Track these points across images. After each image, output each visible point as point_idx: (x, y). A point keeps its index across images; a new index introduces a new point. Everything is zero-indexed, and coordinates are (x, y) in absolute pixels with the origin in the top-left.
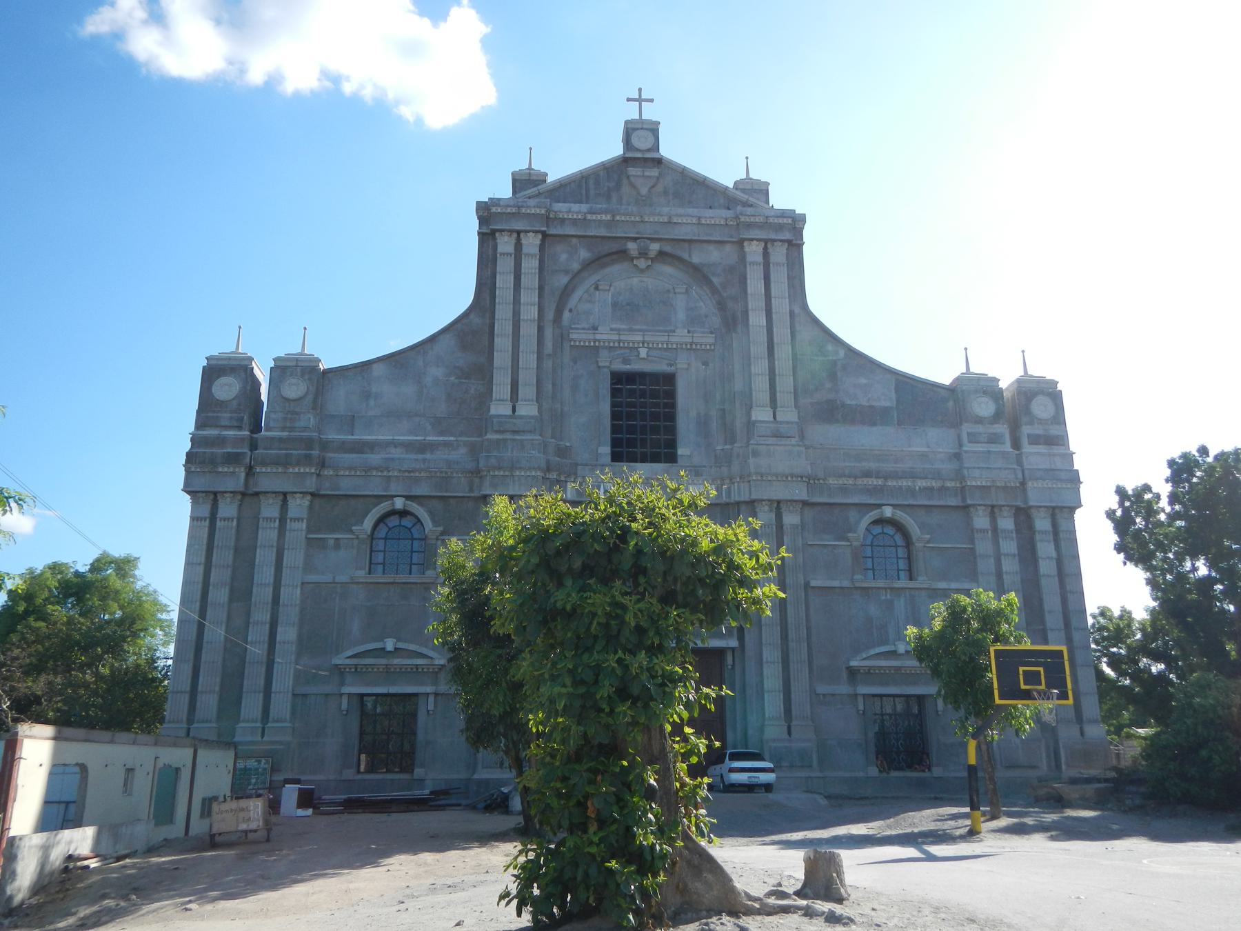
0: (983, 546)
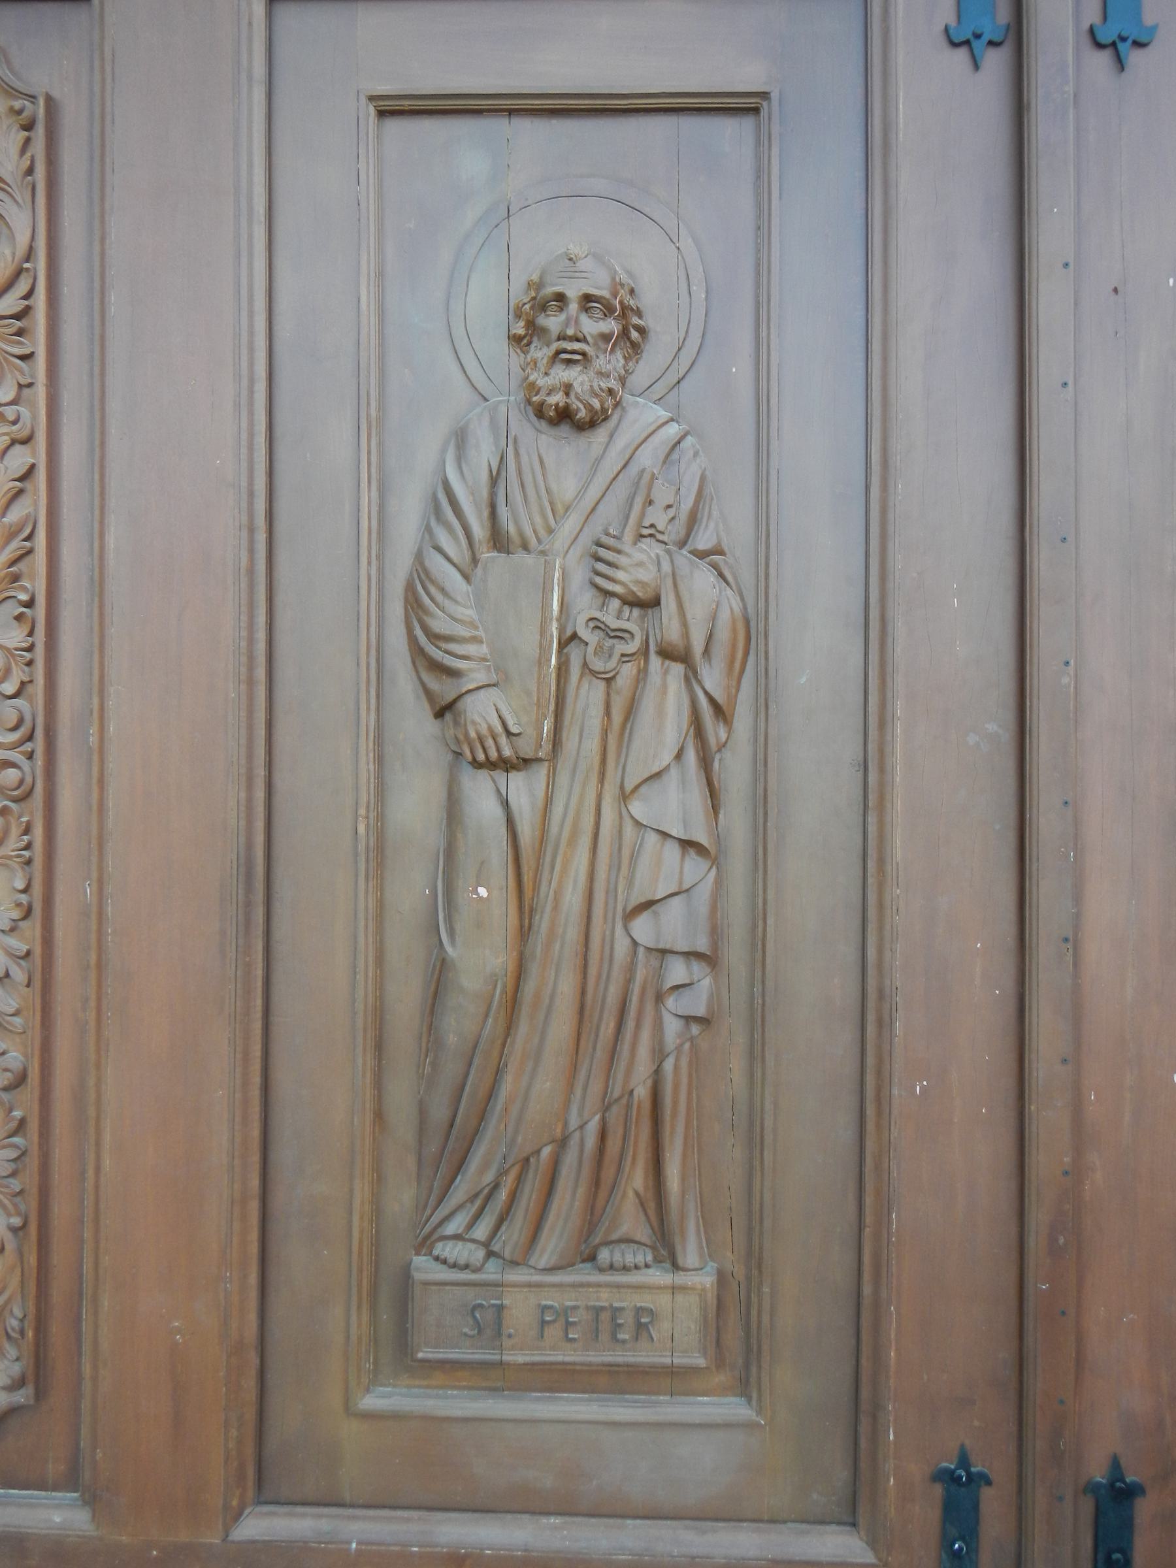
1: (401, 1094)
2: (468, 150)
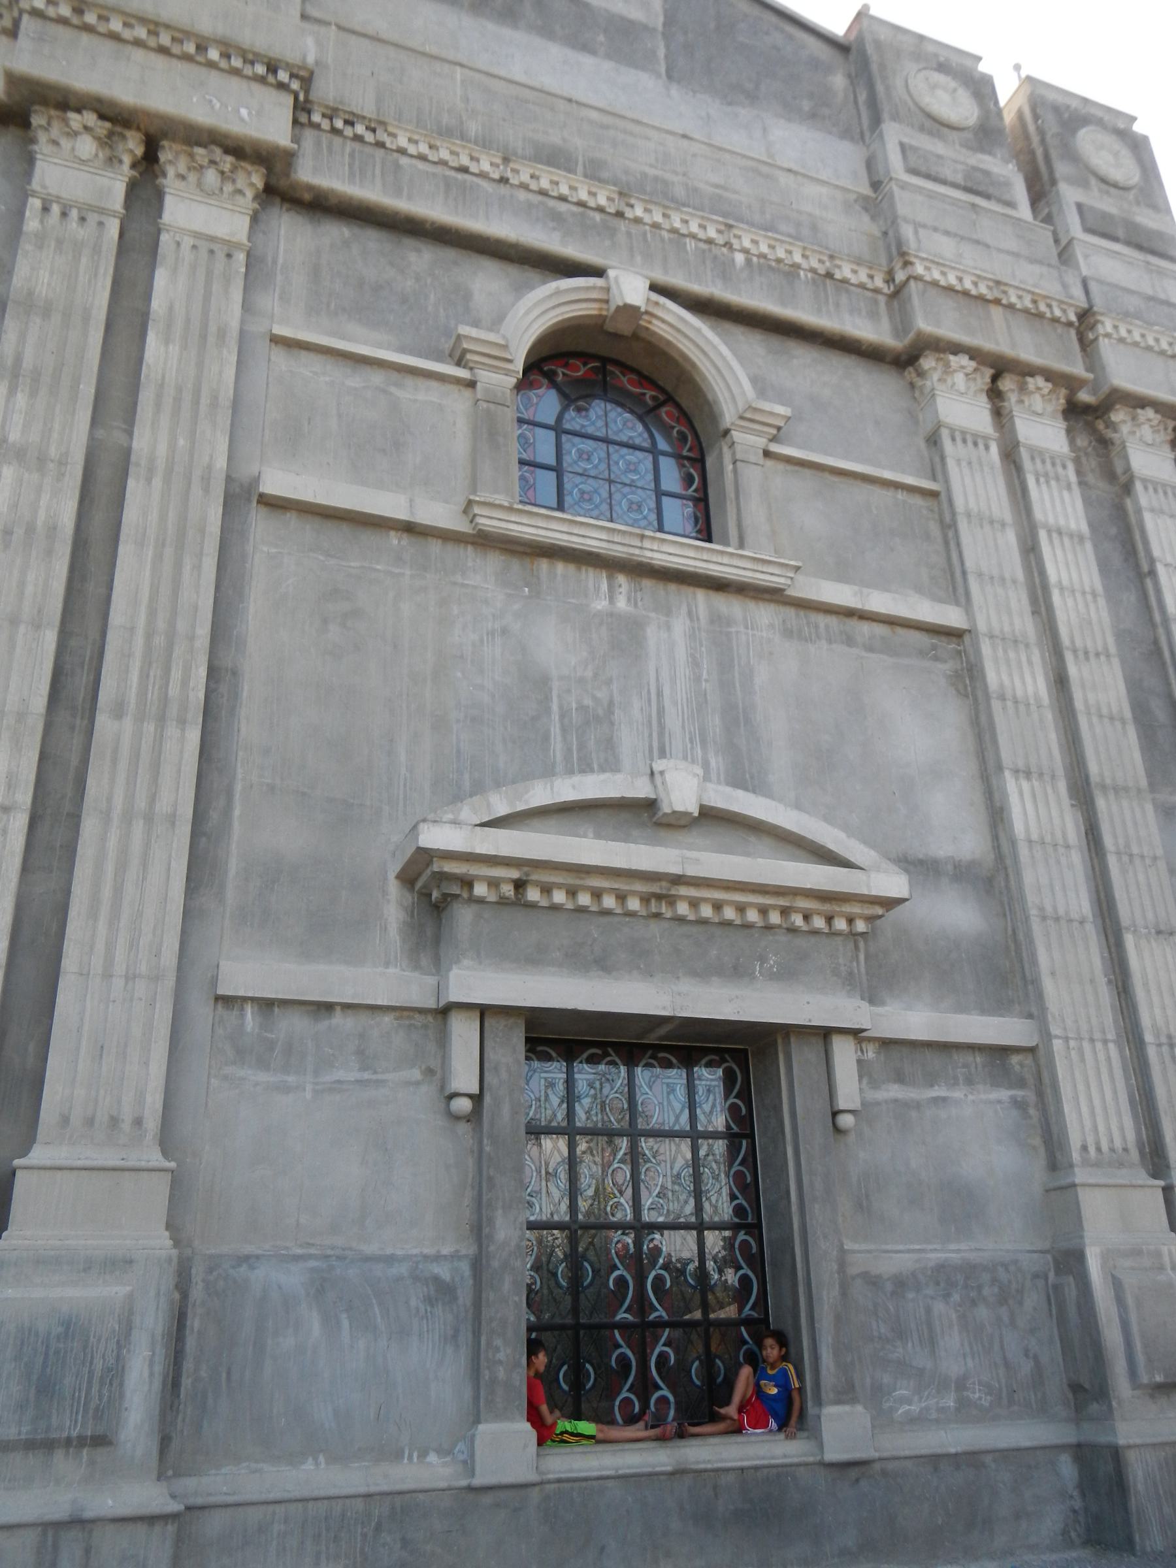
0: (976, 486)
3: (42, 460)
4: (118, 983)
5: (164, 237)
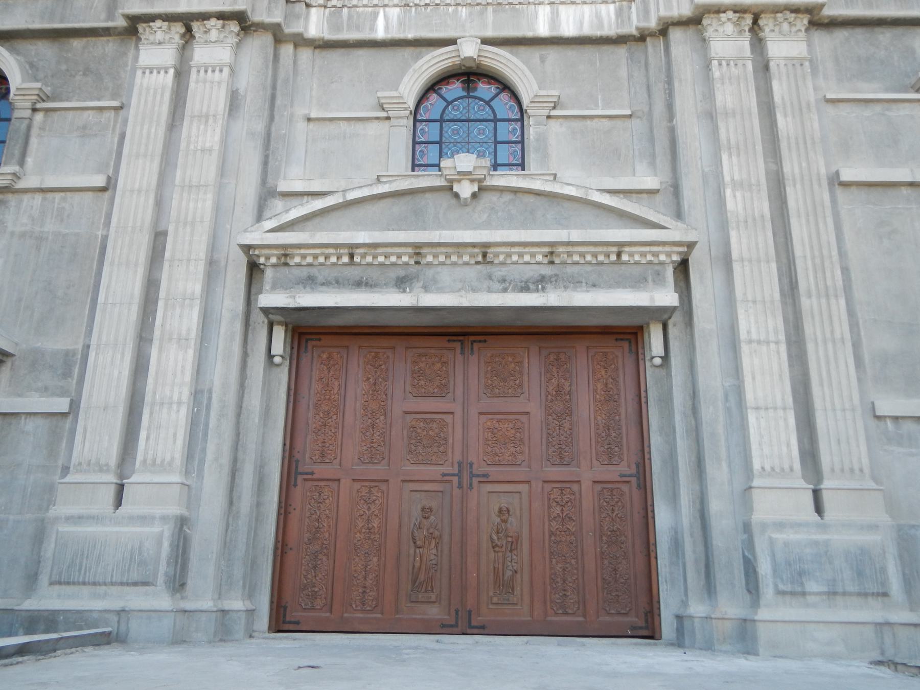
1: (410, 577)
2: (418, 495)
3: (750, 185)
4: (839, 413)
5: (772, 64)
